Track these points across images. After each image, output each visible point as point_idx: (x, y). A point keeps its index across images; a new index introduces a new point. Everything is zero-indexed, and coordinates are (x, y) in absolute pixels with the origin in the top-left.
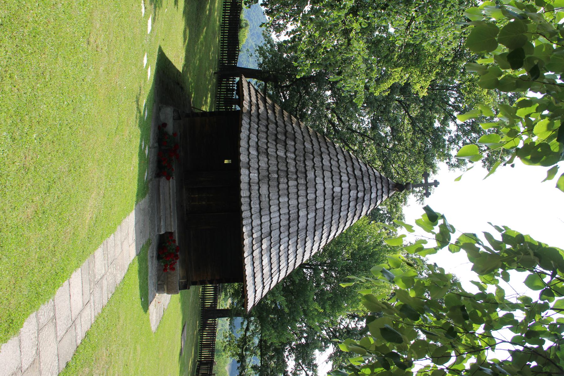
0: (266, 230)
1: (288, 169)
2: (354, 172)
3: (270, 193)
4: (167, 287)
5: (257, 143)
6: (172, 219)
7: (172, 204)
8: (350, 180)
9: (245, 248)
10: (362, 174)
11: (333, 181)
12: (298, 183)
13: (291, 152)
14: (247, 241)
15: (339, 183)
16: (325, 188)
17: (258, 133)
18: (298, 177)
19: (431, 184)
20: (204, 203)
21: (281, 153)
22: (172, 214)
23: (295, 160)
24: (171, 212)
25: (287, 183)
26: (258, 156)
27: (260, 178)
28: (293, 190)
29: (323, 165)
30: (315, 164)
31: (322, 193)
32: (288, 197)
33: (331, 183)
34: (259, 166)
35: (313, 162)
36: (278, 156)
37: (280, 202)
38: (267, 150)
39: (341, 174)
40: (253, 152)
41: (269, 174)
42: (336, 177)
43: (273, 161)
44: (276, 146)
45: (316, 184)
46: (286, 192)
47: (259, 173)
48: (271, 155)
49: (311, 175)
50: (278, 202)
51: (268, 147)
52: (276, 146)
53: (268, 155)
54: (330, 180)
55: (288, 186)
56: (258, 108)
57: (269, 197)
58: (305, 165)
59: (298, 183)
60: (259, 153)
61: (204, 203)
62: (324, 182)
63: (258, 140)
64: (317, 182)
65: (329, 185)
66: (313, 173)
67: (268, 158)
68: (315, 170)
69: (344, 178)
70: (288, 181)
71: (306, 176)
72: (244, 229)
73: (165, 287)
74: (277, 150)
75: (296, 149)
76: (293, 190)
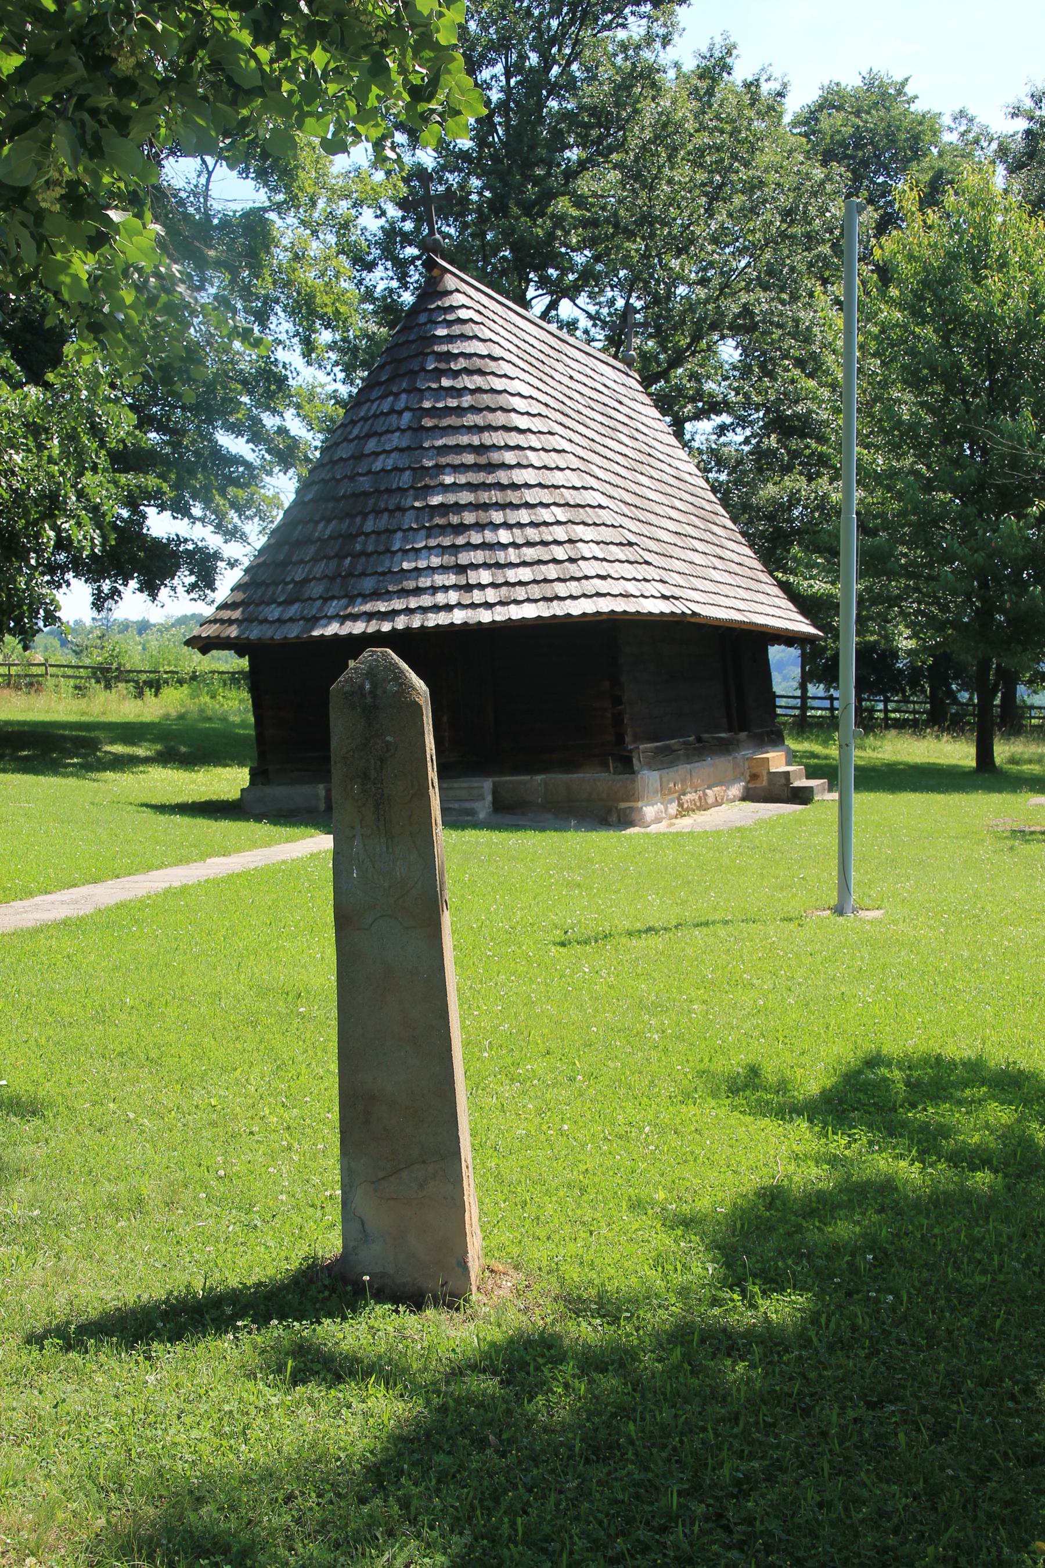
0: (452, 579)
1: (340, 535)
2: (381, 384)
3: (376, 573)
4: (623, 801)
5: (280, 604)
8: (395, 390)
9: (471, 622)
11: (388, 432)
12: (373, 511)
13: (315, 530)
14: (458, 617)
15: (395, 416)
16: (397, 449)
17: (263, 602)
18: (360, 513)
21: (312, 550)
23: (329, 521)
25: (367, 535)
26: (303, 601)
27: (342, 593)
28: (384, 521)
29: (352, 457)
30: (346, 477)
31: (405, 455)
32: (395, 531)
33: (389, 436)
34: (321, 597)
35: (342, 479)
37: (400, 550)
38: (296, 583)
40: (293, 610)
41: (340, 575)
42: (380, 426)
43: (319, 569)
45: (383, 470)
46: (383, 537)
47: (333, 598)
48: (310, 572)
49: (365, 484)
50: (400, 554)
51: (293, 580)
52: (295, 564)
53: (306, 581)
55: (373, 532)
57: (383, 574)
58: (344, 496)
59: (373, 511)
60: (297, 600)
62: (384, 451)
63: (274, 602)
65: (396, 440)
66: (362, 479)
67: (311, 580)
69: (386, 406)
70: (363, 533)
71: (365, 494)
72: (431, 624)
73: (623, 805)
74: (302, 561)
76: (384, 521)
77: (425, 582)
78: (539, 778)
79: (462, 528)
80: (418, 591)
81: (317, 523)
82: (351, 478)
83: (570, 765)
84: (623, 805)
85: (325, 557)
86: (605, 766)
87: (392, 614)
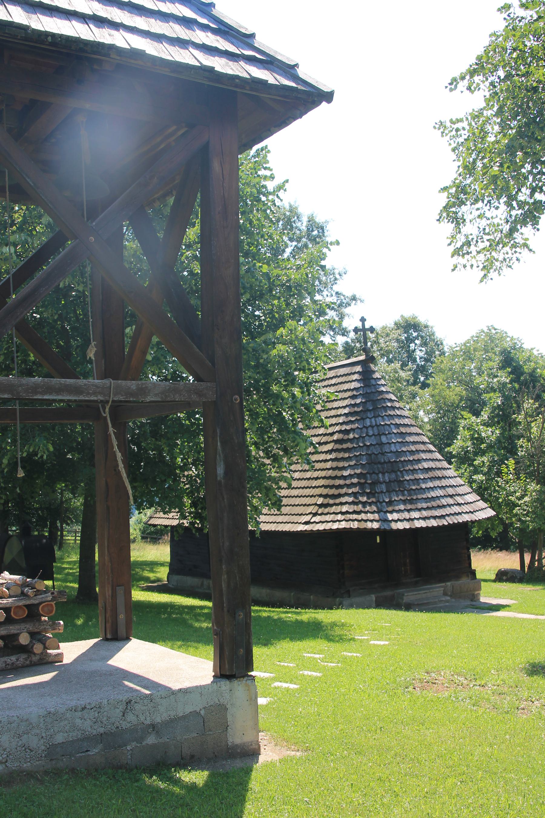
0: (450, 501)
1: (395, 480)
6: (435, 590)
7: (424, 592)
10: (369, 401)
19: (363, 325)
20: (408, 561)
22: (431, 590)
23: (383, 474)
24: (430, 592)
29: (377, 444)
30: (380, 453)
35: (378, 454)
36: (387, 491)
39: (378, 424)
44: (378, 493)
54: (388, 436)
56: (347, 512)
61: (408, 561)
63: (382, 511)
64: (395, 450)
66: (389, 454)
68: (386, 452)
73: (476, 593)
75: (374, 473)
77: (444, 501)
78: (449, 584)
79: (439, 478)
80: (444, 506)
81: (377, 474)
82: (383, 454)
83: (457, 577)
84: (476, 593)
85: (394, 490)
86: (468, 576)
87: (443, 517)
